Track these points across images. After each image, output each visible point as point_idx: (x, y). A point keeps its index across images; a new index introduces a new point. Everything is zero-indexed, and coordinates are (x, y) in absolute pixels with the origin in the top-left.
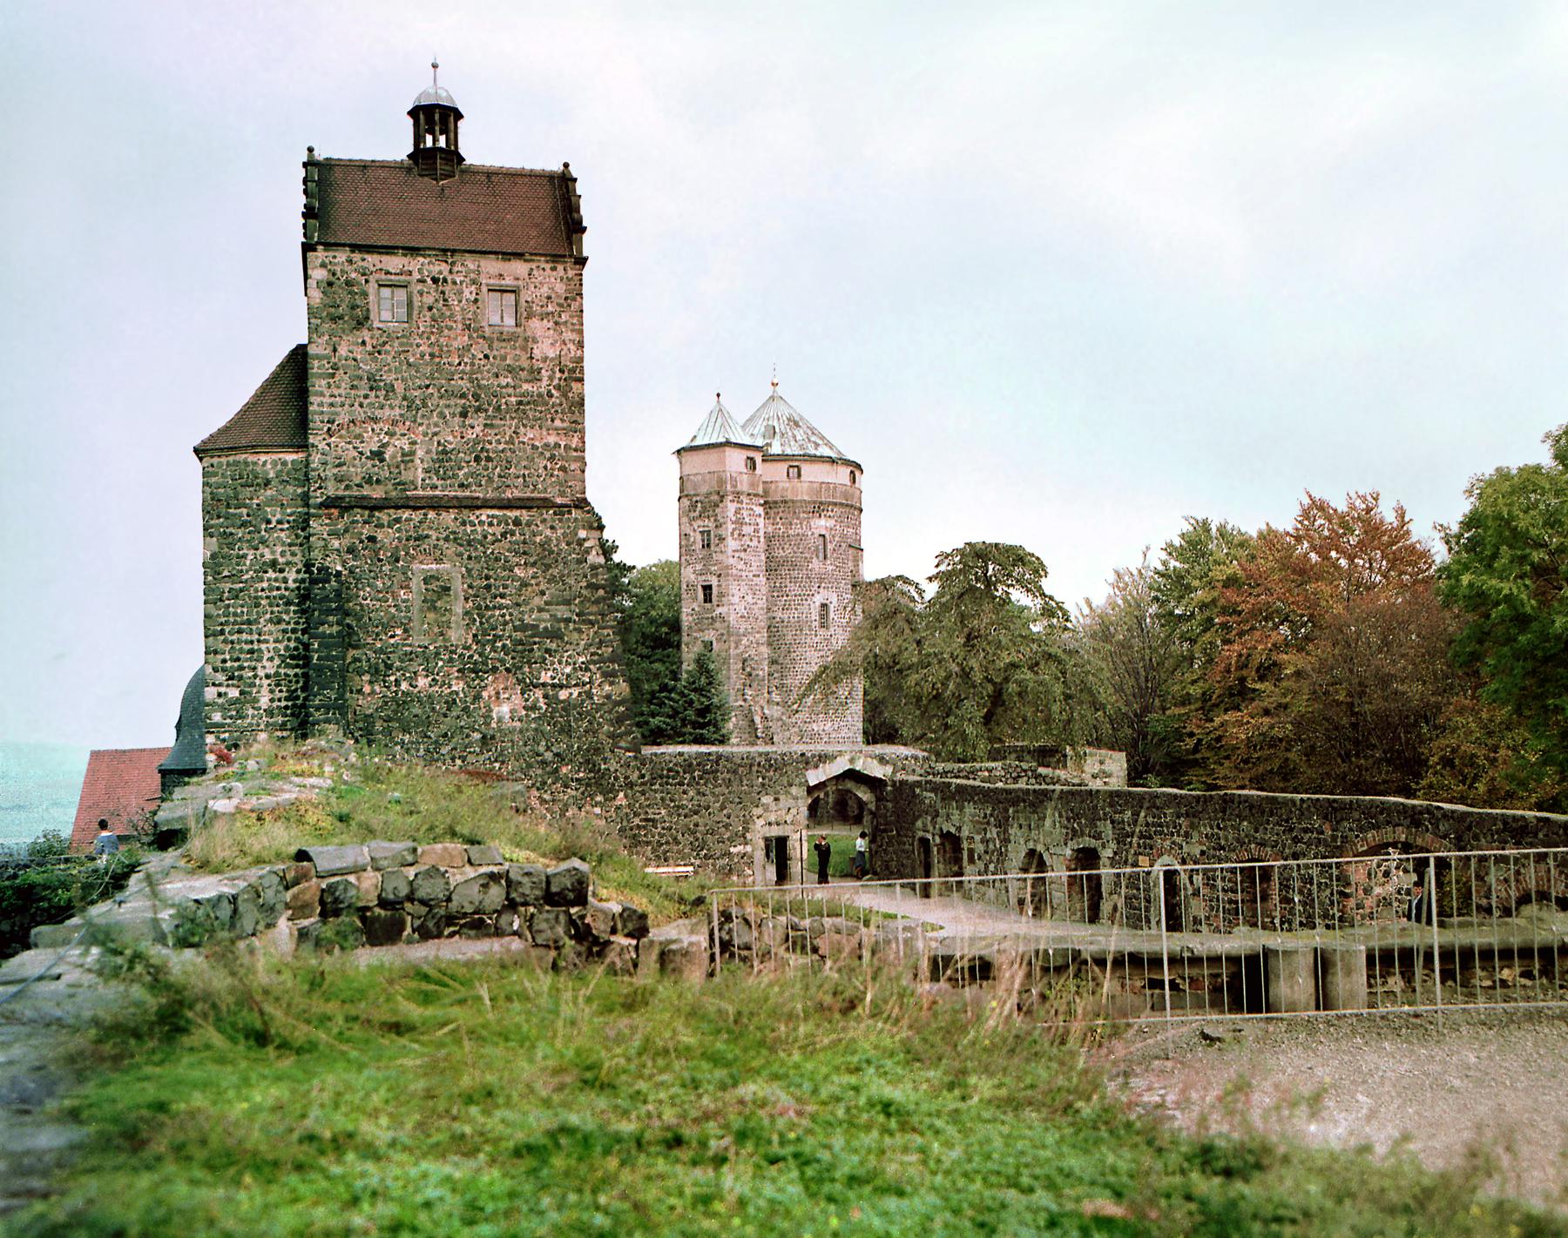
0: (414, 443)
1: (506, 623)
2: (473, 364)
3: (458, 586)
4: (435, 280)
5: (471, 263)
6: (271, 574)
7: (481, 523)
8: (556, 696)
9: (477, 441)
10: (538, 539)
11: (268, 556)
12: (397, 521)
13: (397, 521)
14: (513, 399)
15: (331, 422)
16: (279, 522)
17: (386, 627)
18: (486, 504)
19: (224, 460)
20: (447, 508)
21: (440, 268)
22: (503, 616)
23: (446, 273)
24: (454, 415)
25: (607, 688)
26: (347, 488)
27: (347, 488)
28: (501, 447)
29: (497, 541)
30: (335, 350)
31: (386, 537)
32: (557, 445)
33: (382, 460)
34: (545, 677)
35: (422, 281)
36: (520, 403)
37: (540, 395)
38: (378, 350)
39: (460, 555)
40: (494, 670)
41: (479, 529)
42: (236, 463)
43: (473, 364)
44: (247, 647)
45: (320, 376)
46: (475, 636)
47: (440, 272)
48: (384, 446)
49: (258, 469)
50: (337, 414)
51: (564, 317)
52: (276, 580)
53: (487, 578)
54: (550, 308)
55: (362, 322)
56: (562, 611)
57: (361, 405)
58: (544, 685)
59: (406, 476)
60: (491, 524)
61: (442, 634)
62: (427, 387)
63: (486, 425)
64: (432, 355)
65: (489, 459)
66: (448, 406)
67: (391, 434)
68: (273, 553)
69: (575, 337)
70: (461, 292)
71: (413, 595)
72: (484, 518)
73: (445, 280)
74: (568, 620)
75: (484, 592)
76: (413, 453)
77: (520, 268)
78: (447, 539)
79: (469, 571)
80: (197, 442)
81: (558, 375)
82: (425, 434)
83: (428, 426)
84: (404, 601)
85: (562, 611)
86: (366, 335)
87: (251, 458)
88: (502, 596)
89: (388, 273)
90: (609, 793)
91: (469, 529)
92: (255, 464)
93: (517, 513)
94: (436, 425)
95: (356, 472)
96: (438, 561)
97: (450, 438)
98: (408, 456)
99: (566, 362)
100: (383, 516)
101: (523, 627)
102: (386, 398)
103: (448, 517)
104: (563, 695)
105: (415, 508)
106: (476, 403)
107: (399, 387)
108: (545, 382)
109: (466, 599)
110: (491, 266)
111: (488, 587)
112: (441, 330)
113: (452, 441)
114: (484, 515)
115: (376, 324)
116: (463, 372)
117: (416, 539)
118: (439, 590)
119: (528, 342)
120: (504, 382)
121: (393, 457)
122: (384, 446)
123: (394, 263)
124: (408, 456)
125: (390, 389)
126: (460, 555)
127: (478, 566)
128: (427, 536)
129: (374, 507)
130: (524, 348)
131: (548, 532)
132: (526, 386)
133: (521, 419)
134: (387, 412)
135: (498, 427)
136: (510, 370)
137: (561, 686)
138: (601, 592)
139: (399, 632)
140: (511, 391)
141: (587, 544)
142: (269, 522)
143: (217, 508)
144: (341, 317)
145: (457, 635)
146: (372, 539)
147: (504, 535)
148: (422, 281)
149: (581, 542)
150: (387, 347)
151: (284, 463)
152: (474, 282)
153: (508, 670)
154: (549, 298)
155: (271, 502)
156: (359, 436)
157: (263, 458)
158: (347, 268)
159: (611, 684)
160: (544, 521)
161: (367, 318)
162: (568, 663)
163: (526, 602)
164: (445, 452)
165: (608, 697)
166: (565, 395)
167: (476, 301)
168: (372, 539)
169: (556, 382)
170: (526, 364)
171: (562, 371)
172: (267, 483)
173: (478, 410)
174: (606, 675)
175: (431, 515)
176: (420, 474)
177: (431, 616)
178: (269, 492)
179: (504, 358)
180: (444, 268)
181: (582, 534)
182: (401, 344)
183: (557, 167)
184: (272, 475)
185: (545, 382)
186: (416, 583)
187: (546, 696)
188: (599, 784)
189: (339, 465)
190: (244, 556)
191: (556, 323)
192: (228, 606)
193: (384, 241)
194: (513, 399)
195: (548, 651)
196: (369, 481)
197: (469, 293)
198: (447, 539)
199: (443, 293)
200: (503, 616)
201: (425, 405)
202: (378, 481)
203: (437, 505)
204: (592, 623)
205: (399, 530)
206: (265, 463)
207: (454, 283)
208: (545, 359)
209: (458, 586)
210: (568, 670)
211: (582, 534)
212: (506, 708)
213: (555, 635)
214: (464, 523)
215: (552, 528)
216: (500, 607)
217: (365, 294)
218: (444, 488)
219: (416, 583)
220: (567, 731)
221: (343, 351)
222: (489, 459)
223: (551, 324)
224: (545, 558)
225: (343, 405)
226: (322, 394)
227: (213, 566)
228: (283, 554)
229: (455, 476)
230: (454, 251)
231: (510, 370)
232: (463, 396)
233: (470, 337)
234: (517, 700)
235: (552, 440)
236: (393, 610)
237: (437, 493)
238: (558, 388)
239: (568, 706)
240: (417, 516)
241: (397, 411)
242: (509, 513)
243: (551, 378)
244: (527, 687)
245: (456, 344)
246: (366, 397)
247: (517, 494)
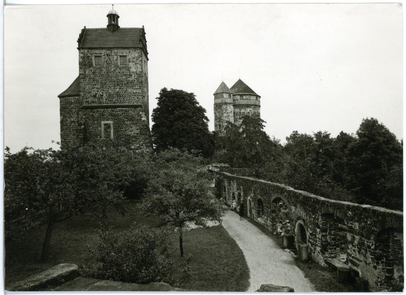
0: (103, 93)
1: (123, 135)
2: (116, 74)
3: (112, 126)
4: (107, 55)
6: (73, 124)
7: (117, 111)
8: (135, 152)
9: (118, 92)
10: (130, 114)
11: (72, 120)
12: (98, 111)
13: (98, 111)
14: (126, 82)
15: (84, 89)
16: (75, 112)
17: (96, 136)
18: (119, 107)
19: (64, 99)
20: (109, 108)
22: (123, 133)
23: (110, 53)
24: (112, 86)
25: (147, 150)
26: (88, 104)
27: (88, 104)
28: (123, 93)
29: (121, 115)
30: (85, 73)
31: (96, 115)
32: (136, 92)
33: (96, 97)
34: (133, 147)
35: (104, 55)
36: (127, 83)
37: (132, 81)
38: (94, 73)
39: (113, 119)
40: (121, 145)
41: (117, 112)
42: (66, 99)
43: (116, 74)
44: (68, 141)
45: (82, 78)
46: (116, 138)
47: (108, 53)
48: (97, 94)
49: (70, 100)
50: (86, 87)
51: (138, 62)
52: (74, 125)
53: (119, 124)
54: (134, 60)
55: (91, 65)
57: (91, 85)
58: (133, 149)
59: (101, 100)
60: (119, 111)
61: (108, 137)
62: (106, 80)
63: (119, 88)
64: (107, 73)
65: (120, 96)
66: (111, 84)
67: (98, 91)
68: (73, 119)
69: (140, 66)
70: (113, 58)
72: (118, 110)
73: (110, 55)
74: (137, 134)
76: (103, 95)
77: (127, 51)
78: (109, 115)
79: (114, 122)
80: (59, 95)
81: (136, 76)
82: (106, 91)
83: (106, 89)
84: (100, 130)
86: (92, 68)
87: (69, 98)
88: (122, 128)
89: (97, 54)
91: (114, 112)
92: (69, 99)
93: (126, 109)
94: (108, 89)
96: (108, 120)
97: (112, 92)
99: (138, 72)
100: (95, 110)
101: (128, 135)
102: (97, 83)
103: (109, 110)
104: (137, 151)
105: (102, 108)
106: (119, 83)
107: (100, 80)
108: (133, 77)
109: (114, 129)
111: (119, 126)
112: (109, 66)
114: (118, 109)
115: (94, 66)
116: (114, 76)
117: (102, 115)
118: (107, 126)
119: (129, 69)
120: (123, 78)
121: (98, 96)
122: (97, 94)
123: (97, 51)
125: (97, 81)
126: (113, 119)
127: (116, 121)
128: (105, 115)
129: (92, 108)
130: (128, 70)
131: (133, 113)
132: (129, 79)
133: (128, 87)
134: (97, 86)
135: (123, 88)
136: (125, 75)
137: (136, 149)
138: (145, 127)
139: (99, 137)
140: (125, 80)
141: (142, 115)
142: (72, 112)
143: (63, 109)
144: (86, 65)
146: (92, 115)
147: (122, 114)
148: (104, 55)
149: (140, 115)
150: (97, 71)
151: (75, 99)
152: (116, 55)
153: (124, 146)
154: (134, 58)
155: (72, 108)
156: (91, 92)
157: (71, 98)
158: (88, 53)
159: (148, 149)
160: (132, 110)
161: (92, 65)
162: (138, 144)
163: (128, 130)
164: (110, 95)
165: (148, 152)
166: (138, 81)
167: (117, 59)
168: (92, 115)
169: (136, 77)
170: (128, 73)
171: (137, 75)
172: (72, 103)
173: (118, 85)
174: (147, 146)
175: (106, 109)
176: (105, 100)
177: (106, 133)
178: (72, 106)
179: (123, 72)
180: (109, 52)
181: (141, 113)
182: (100, 70)
183: (141, 27)
184: (73, 101)
185: (133, 77)
186: (103, 126)
187: (133, 151)
189: (87, 99)
190: (68, 120)
191: (136, 64)
192: (65, 132)
193: (96, 46)
194: (126, 82)
195: (133, 141)
196: (93, 102)
197: (115, 58)
198: (109, 115)
199: (109, 58)
200: (123, 133)
201: (105, 84)
202: (95, 102)
204: (143, 134)
205: (99, 113)
206: (71, 99)
207: (112, 55)
208: (133, 72)
209: (112, 126)
210: (138, 145)
211: (141, 113)
214: (113, 111)
215: (134, 112)
216: (122, 131)
217: (91, 59)
218: (110, 103)
219: (103, 126)
221: (87, 72)
222: (120, 96)
223: (134, 64)
224: (132, 119)
225: (87, 85)
226: (82, 83)
227: (62, 122)
228: (75, 119)
229: (113, 101)
230: (111, 48)
231: (125, 75)
232: (114, 82)
233: (116, 68)
235: (135, 91)
236: (97, 132)
237: (109, 104)
238: (136, 79)
240: (102, 110)
241: (99, 86)
242: (124, 109)
243: (135, 77)
245: (112, 70)
246: (92, 83)
247: (127, 104)
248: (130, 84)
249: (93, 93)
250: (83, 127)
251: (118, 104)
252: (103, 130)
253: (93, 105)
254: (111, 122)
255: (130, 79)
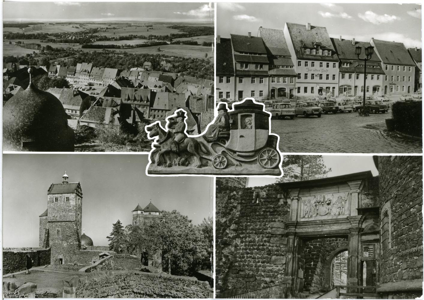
5: (64, 194)
21: (61, 195)
31: (54, 225)
55: (53, 202)
56: (71, 234)
71: (56, 232)
75: (63, 231)
77: (69, 194)
85: (71, 234)
90: (76, 255)
95: (52, 218)
98: (57, 216)
100: (53, 223)
103: (60, 223)
106: (65, 210)
110: (66, 195)
113: (61, 214)
118: (58, 231)
124: (57, 216)
129: (52, 222)
145: (60, 236)
186: (56, 231)
188: (75, 254)
203: (59, 222)
212: (65, 245)
213: (70, 236)
220: (71, 247)
224: (69, 228)
234: (66, 244)
235: (72, 214)
239: (72, 245)
244: (67, 242)
248: (70, 211)
249: (53, 215)
250: (47, 231)
251: (64, 220)
252: (56, 233)
253: (53, 220)
254: (60, 229)
255: (70, 208)
